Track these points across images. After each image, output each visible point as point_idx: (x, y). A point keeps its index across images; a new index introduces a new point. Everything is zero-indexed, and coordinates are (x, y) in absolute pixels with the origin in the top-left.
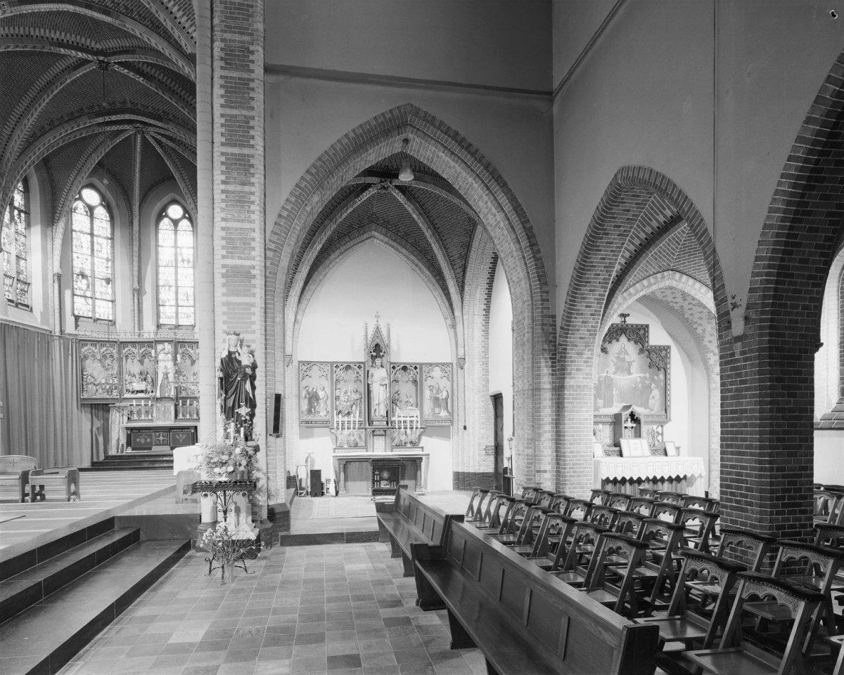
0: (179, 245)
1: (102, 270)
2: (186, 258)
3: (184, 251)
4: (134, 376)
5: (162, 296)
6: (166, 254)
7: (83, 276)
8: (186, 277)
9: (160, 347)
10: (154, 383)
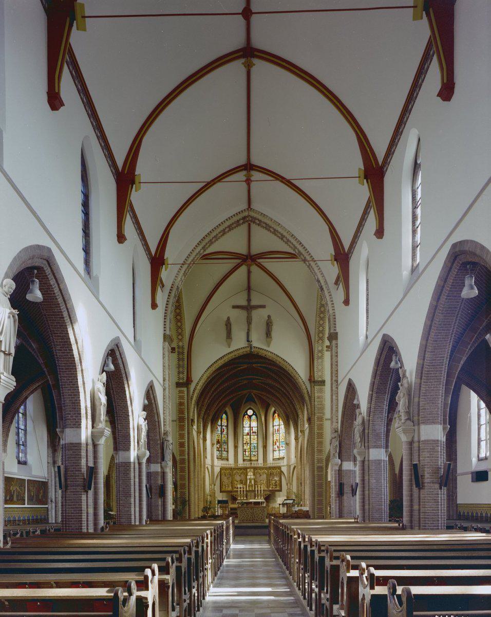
4: (237, 482)
5: (245, 447)
6: (247, 430)
9: (248, 470)
10: (246, 484)
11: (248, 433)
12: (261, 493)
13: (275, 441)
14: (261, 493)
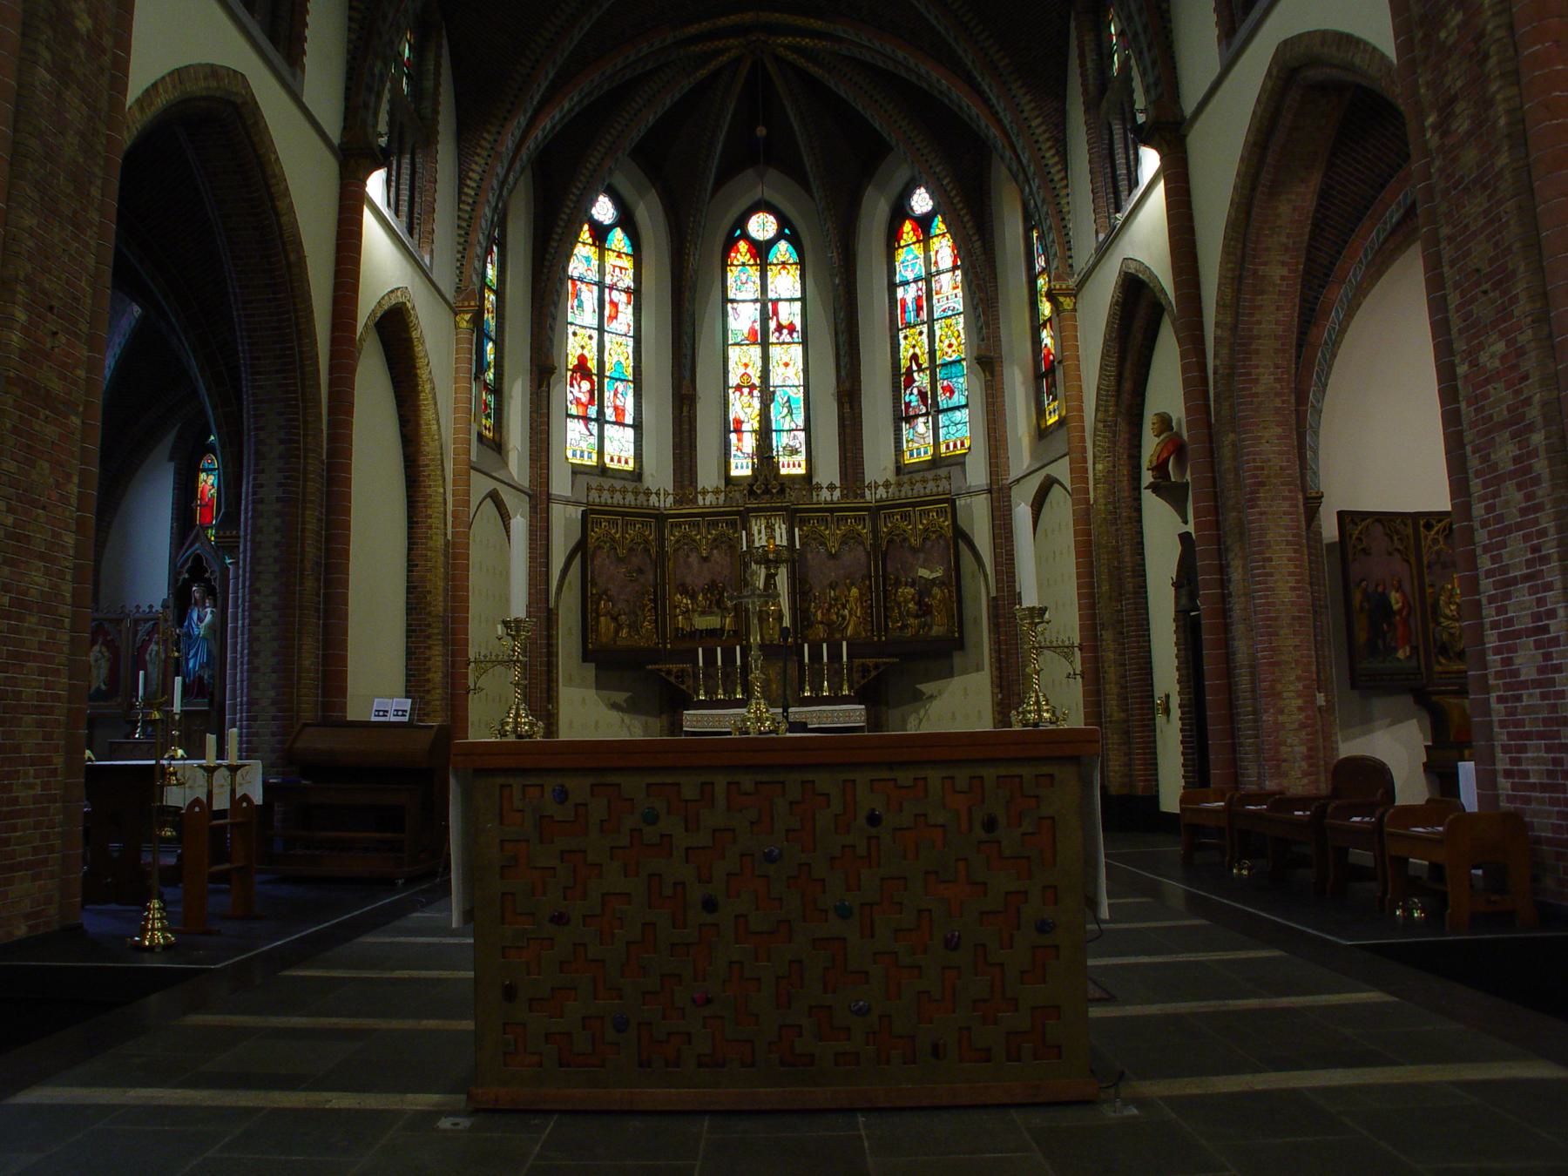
0: (771, 295)
1: (620, 354)
2: (785, 322)
3: (782, 306)
6: (743, 319)
7: (582, 369)
8: (786, 365)
11: (753, 332)
12: (835, 655)
13: (904, 363)
14: (835, 655)
